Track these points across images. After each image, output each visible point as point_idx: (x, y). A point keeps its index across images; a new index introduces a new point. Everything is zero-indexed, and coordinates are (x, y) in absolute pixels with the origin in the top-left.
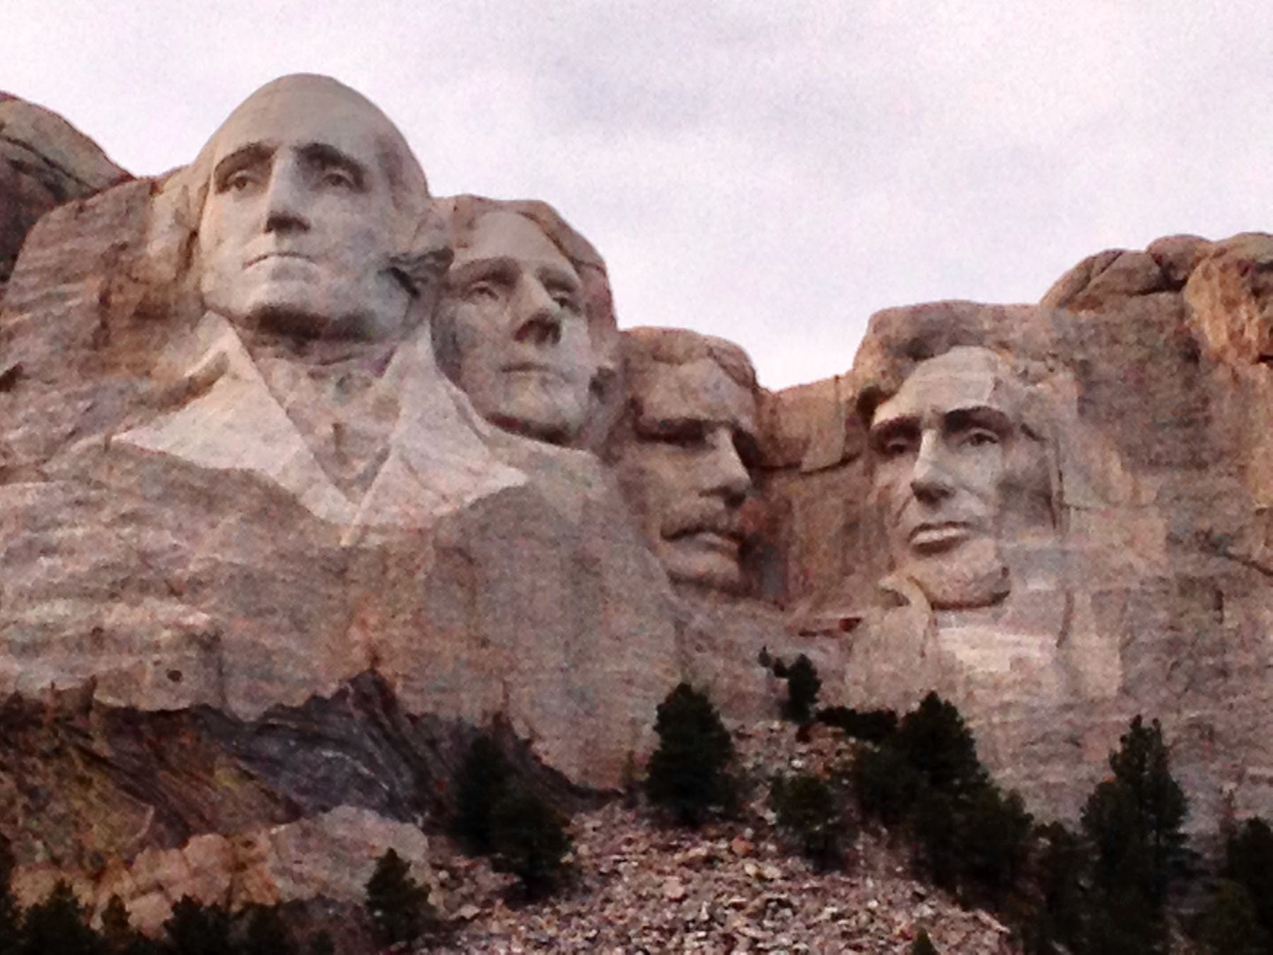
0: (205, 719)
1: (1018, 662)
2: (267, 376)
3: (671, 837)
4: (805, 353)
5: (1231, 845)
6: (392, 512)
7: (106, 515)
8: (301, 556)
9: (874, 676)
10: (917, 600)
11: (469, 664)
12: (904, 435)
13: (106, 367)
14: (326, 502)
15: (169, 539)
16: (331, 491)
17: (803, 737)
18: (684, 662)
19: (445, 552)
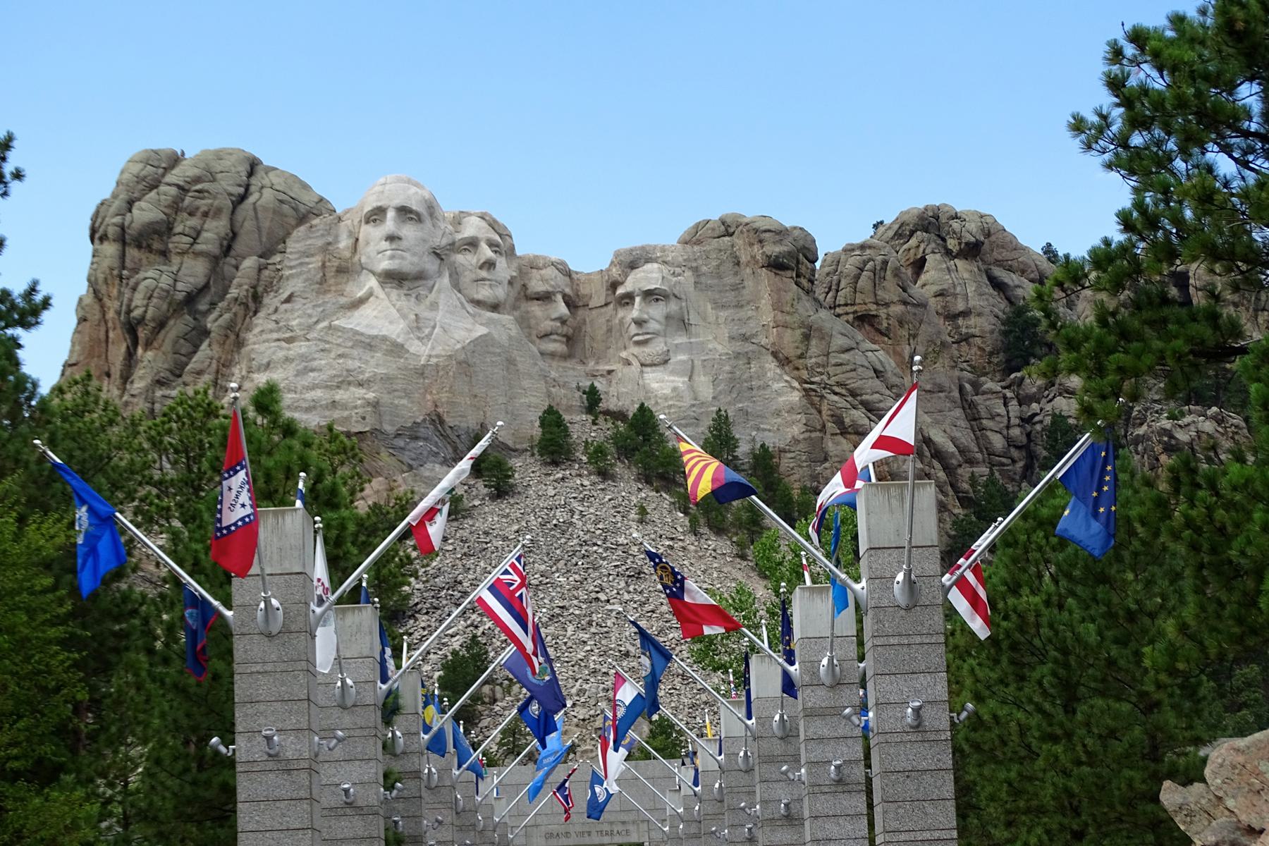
0: (376, 432)
1: (675, 389)
2: (388, 295)
3: (549, 469)
4: (590, 260)
5: (755, 457)
6: (439, 350)
7: (333, 355)
8: (406, 369)
9: (621, 396)
10: (636, 363)
11: (471, 405)
12: (628, 299)
13: (326, 292)
14: (414, 347)
15: (357, 364)
16: (416, 342)
17: (594, 423)
18: (549, 395)
19: (459, 363)
